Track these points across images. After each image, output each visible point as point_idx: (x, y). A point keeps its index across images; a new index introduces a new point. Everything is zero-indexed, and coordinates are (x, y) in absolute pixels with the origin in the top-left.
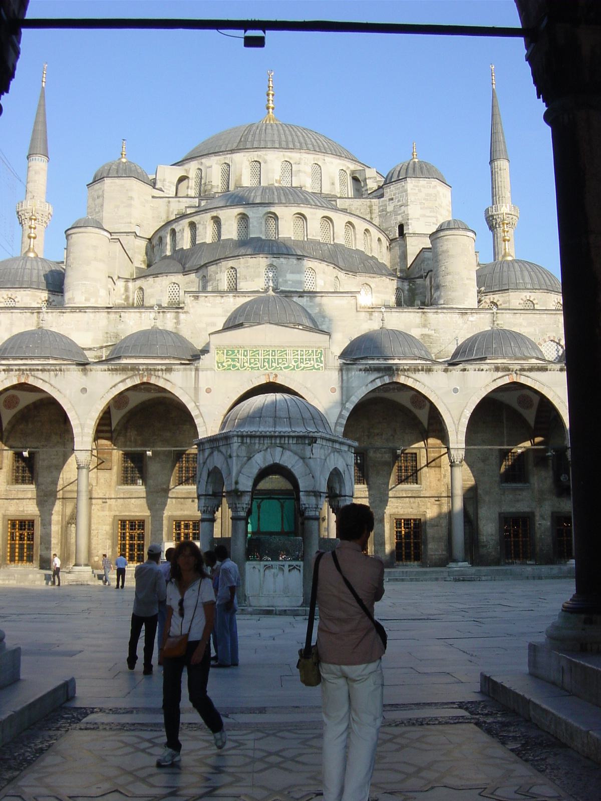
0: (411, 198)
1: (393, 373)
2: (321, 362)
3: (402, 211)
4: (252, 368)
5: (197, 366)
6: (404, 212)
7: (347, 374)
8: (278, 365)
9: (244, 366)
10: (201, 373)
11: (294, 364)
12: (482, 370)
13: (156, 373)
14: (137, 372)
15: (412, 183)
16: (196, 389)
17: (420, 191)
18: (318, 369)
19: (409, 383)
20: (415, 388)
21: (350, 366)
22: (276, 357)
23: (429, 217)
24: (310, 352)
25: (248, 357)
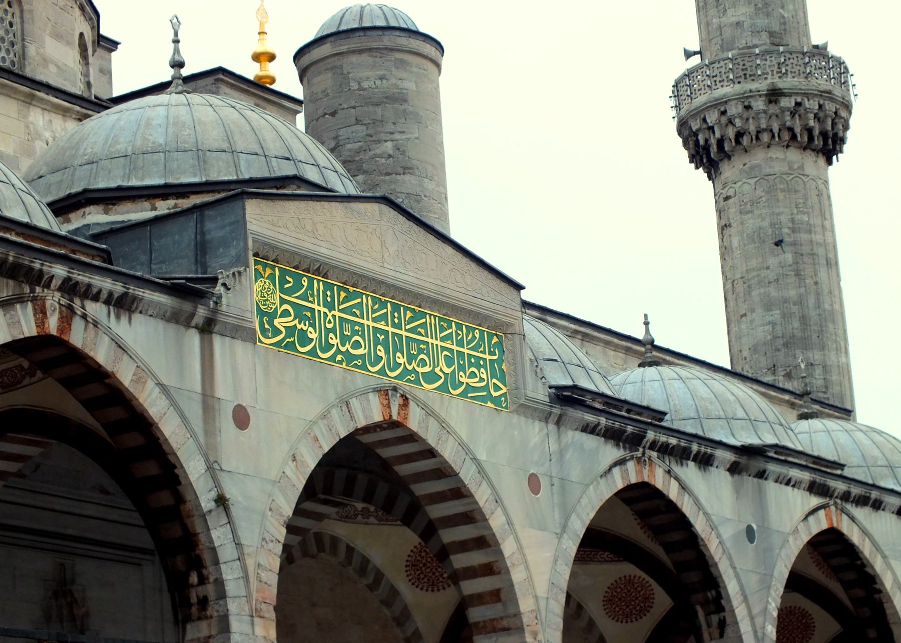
5: (215, 311)
7: (559, 437)
10: (218, 343)
14: (27, 290)
18: (496, 401)
19: (673, 492)
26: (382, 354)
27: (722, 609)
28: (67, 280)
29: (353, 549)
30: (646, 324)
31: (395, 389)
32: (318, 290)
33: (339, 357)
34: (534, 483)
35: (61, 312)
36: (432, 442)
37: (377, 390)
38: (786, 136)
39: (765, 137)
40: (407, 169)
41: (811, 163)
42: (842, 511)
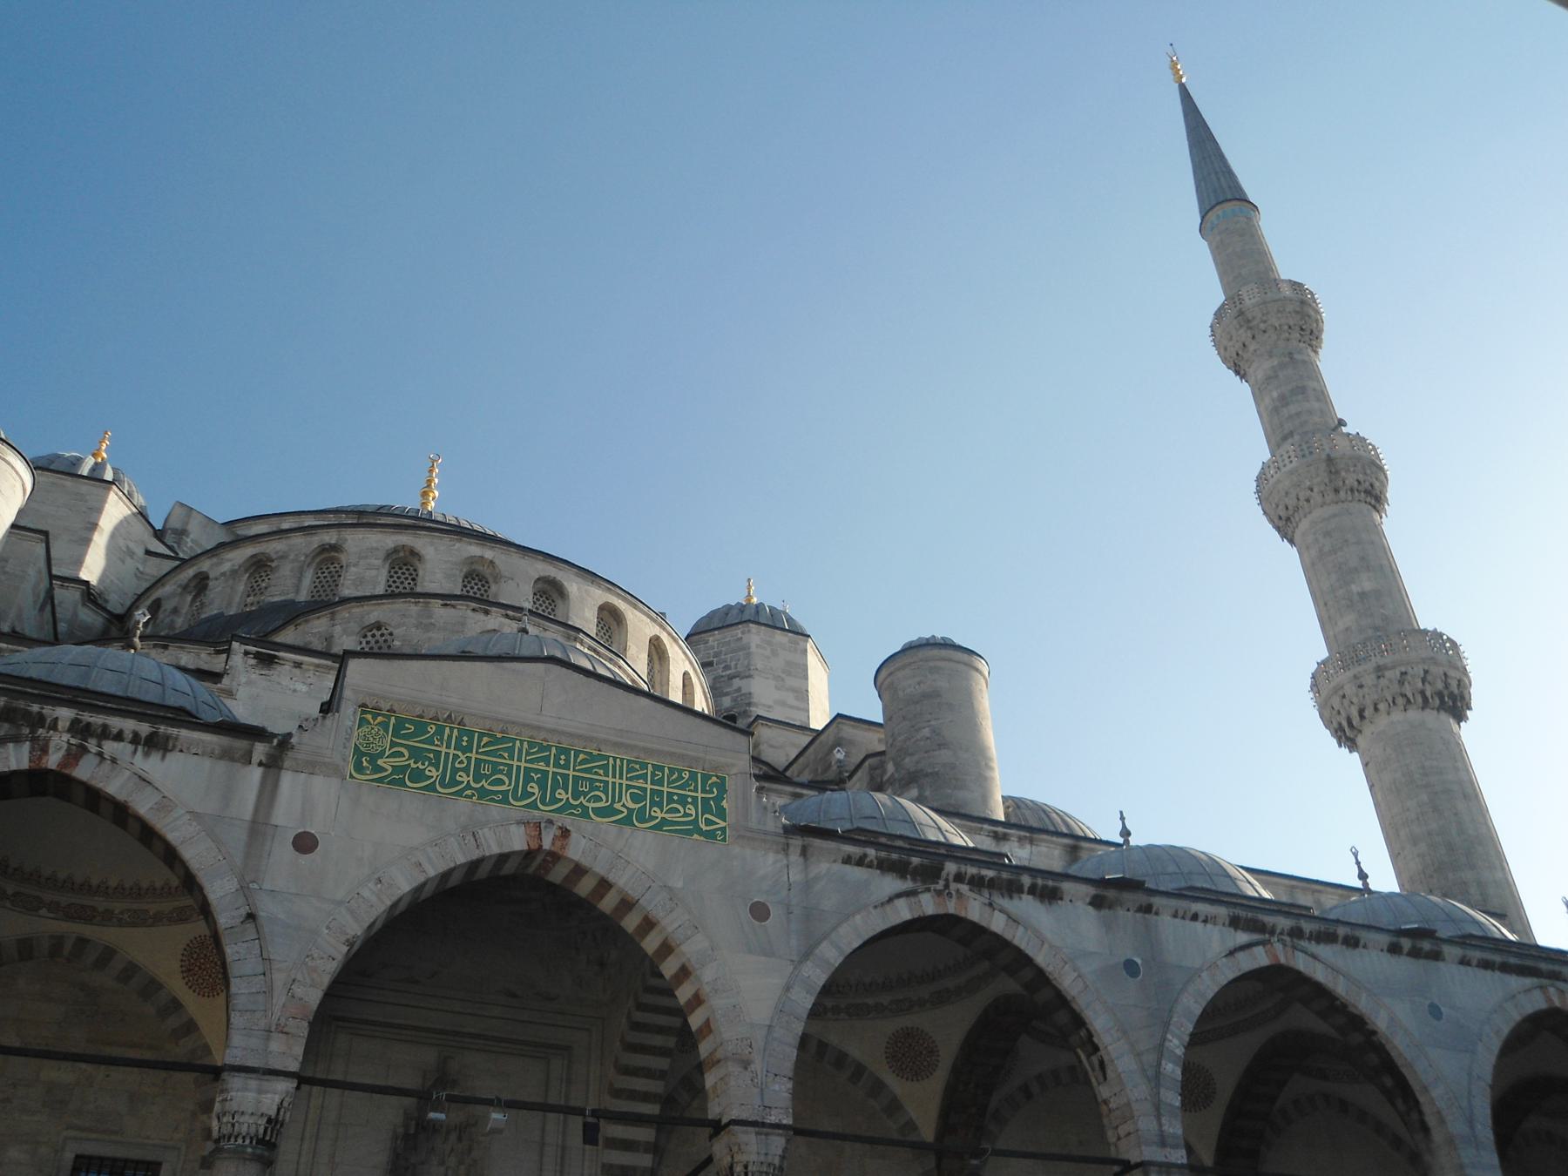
0: (759, 666)
1: (947, 886)
2: (721, 814)
3: (735, 687)
4: (483, 793)
6: (739, 689)
7: (806, 868)
8: (576, 796)
9: (455, 783)
10: (287, 779)
11: (631, 805)
12: (1195, 917)
13: (109, 747)
14: (26, 731)
15: (758, 633)
16: (259, 828)
17: (774, 653)
18: (710, 835)
19: (997, 924)
20: (1016, 942)
21: (817, 842)
22: (571, 773)
23: (791, 707)
24: (686, 776)
25: (473, 756)
26: (536, 790)
27: (1096, 1049)
28: (75, 722)
29: (827, 1045)
30: (1122, 818)
31: (550, 822)
32: (450, 737)
33: (469, 792)
34: (760, 912)
35: (68, 750)
36: (600, 868)
37: (526, 824)
38: (1400, 701)
39: (1382, 706)
40: (941, 746)
41: (1431, 718)
42: (1294, 948)
